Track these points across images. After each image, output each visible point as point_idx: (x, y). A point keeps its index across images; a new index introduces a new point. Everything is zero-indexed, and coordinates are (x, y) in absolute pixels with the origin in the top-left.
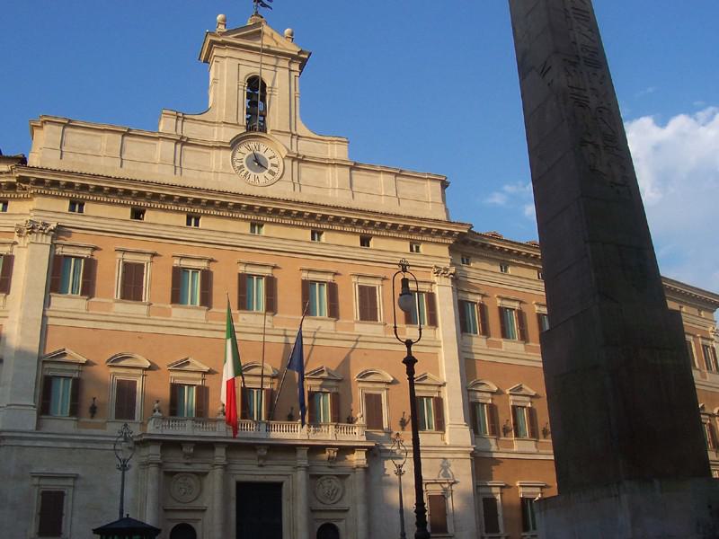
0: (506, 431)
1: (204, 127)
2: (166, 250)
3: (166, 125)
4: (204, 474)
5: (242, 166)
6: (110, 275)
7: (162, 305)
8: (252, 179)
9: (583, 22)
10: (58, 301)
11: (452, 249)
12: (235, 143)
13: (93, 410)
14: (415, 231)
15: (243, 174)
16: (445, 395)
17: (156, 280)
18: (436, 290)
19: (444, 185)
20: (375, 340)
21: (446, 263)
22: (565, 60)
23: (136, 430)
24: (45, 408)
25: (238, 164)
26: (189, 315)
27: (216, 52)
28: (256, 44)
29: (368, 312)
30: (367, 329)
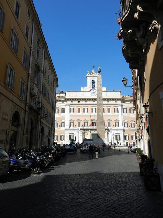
0: (129, 126)
1: (86, 89)
2: (82, 106)
3: (82, 89)
4: (88, 133)
6: (76, 110)
10: (70, 113)
11: (121, 101)
12: (91, 90)
13: (75, 126)
14: (116, 100)
16: (119, 122)
17: (82, 110)
18: (118, 107)
19: (121, 92)
21: (120, 104)
23: (79, 128)
24: (70, 126)
26: (86, 114)
27: (88, 77)
28: (93, 75)
30: (109, 114)
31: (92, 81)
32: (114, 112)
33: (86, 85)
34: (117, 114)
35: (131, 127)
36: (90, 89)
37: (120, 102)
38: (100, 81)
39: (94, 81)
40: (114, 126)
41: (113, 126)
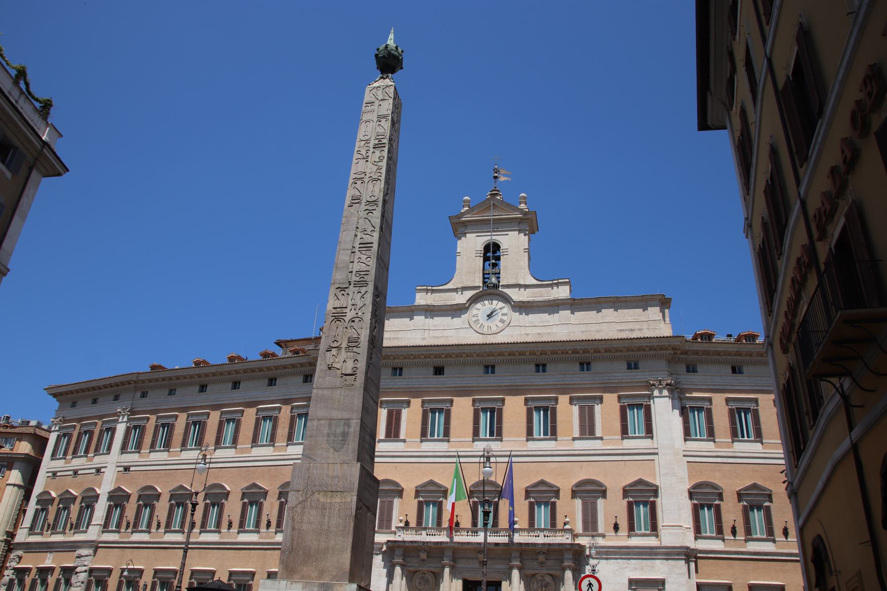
5: (478, 320)
7: (414, 440)
8: (486, 328)
9: (364, 252)
11: (670, 362)
12: (474, 300)
15: (478, 326)
20: (592, 452)
22: (339, 288)
25: (474, 319)
29: (588, 429)
31: (487, 248)
32: (624, 431)
33: (449, 272)
34: (645, 444)
35: (748, 531)
36: (469, 294)
37: (663, 364)
38: (380, 117)
39: (496, 247)
40: (624, 524)
41: (616, 528)
